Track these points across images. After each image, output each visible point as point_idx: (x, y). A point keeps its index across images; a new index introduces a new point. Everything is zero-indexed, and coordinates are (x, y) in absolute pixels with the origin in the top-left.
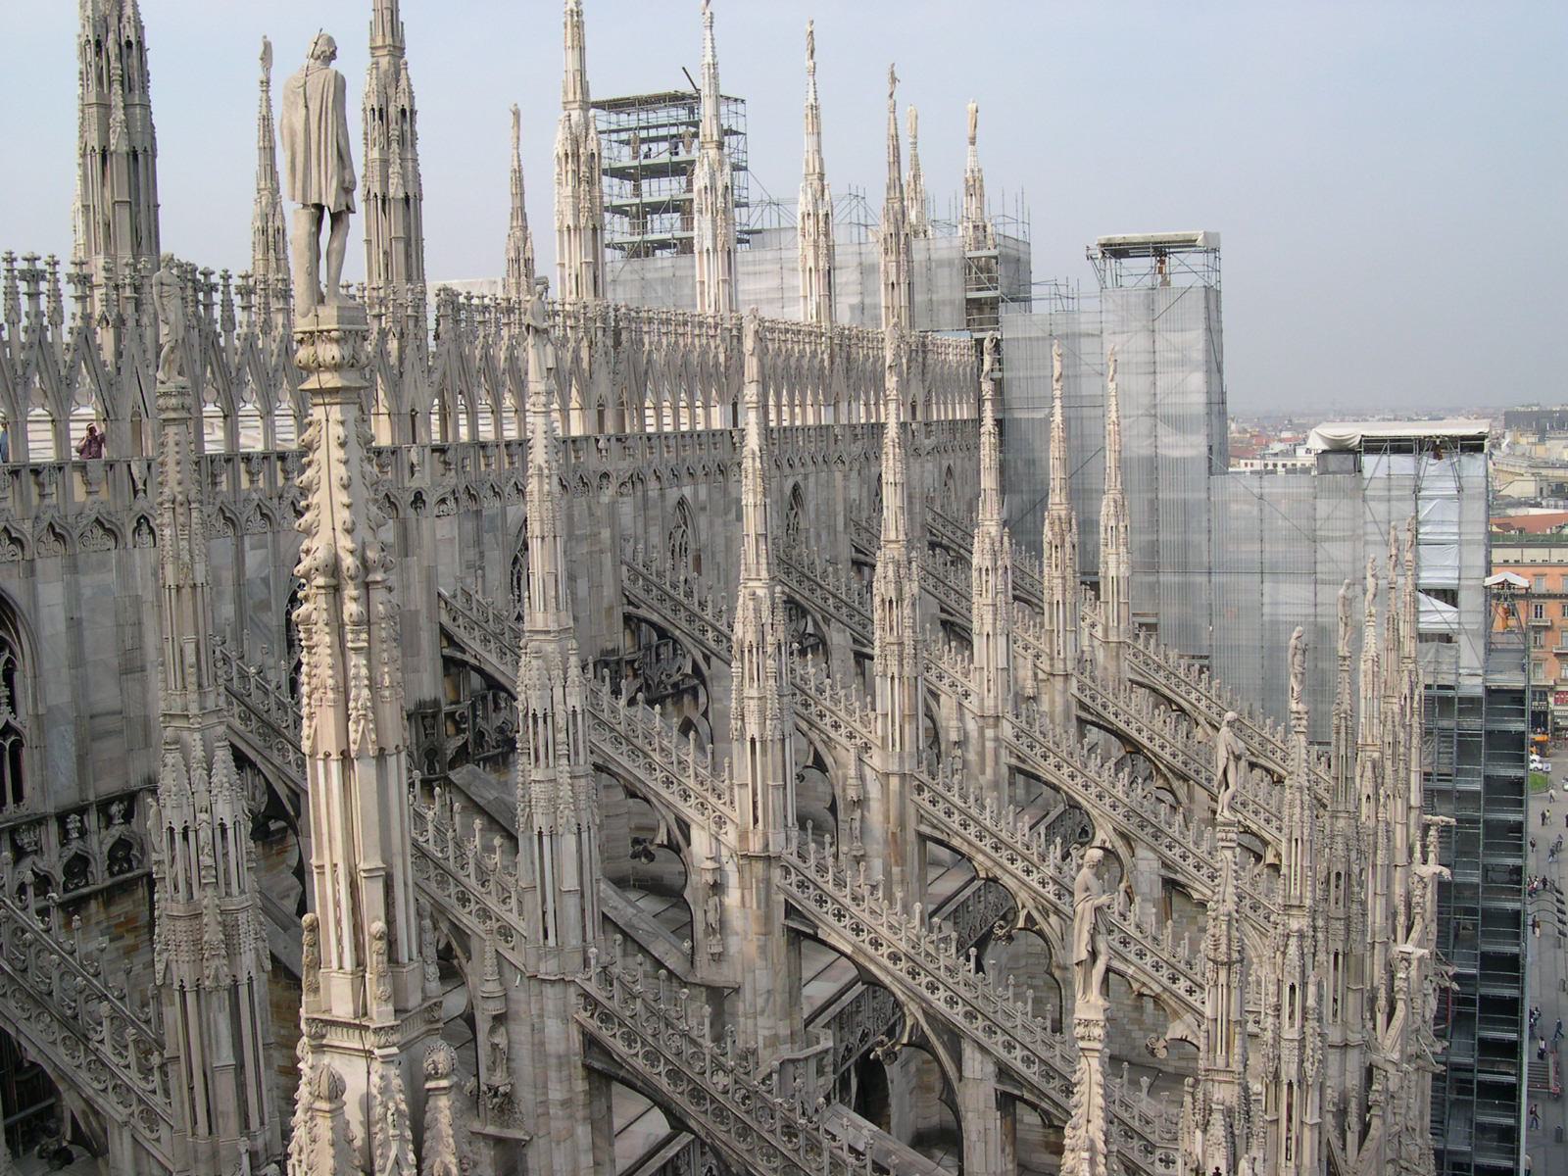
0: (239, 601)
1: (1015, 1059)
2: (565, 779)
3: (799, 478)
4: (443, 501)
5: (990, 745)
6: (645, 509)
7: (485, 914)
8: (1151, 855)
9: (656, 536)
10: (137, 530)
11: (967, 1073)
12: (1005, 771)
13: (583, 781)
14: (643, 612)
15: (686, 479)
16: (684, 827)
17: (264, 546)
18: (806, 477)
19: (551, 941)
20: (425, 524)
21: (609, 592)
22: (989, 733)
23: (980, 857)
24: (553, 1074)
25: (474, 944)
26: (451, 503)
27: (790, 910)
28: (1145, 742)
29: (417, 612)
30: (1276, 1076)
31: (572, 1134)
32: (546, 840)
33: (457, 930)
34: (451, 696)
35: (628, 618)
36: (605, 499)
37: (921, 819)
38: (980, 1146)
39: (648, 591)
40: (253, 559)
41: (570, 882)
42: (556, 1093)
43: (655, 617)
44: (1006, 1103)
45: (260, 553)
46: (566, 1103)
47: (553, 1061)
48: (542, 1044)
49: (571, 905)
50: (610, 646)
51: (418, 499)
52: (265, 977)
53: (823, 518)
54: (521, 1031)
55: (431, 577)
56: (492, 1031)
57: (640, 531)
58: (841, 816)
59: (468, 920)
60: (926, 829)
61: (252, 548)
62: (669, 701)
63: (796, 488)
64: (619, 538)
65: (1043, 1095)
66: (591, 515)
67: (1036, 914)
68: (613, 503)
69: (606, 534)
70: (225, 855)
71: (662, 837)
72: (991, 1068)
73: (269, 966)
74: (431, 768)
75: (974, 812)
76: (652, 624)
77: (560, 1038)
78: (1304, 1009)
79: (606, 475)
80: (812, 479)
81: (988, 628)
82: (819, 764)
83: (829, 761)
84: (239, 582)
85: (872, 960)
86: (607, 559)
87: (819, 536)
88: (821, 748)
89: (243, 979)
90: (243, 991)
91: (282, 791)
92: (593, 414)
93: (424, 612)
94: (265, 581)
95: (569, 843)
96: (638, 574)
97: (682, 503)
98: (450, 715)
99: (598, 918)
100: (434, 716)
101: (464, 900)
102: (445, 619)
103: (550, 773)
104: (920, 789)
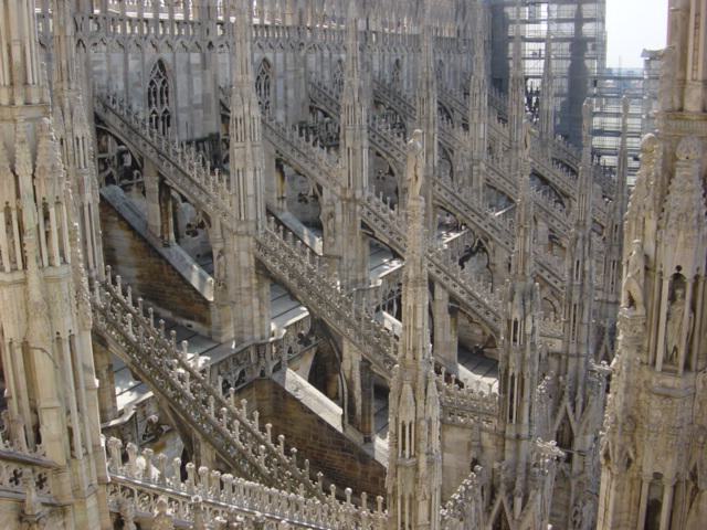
0: (126, 81)
1: (457, 290)
2: (248, 146)
3: (400, 58)
4: (222, 46)
5: (475, 173)
6: (322, 61)
7: (216, 207)
8: (543, 224)
9: (326, 73)
10: (78, 45)
11: (437, 297)
12: (481, 185)
13: (258, 148)
14: (318, 105)
15: (343, 51)
16: (320, 188)
17: (137, 59)
18: (403, 57)
19: (243, 218)
20: (213, 55)
21: (303, 96)
22: (475, 168)
23: (459, 215)
24: (243, 276)
25: (212, 220)
26: (225, 47)
27: (364, 225)
28: (550, 179)
29: (209, 95)
30: (570, 302)
31: (251, 303)
32: (241, 173)
33: (205, 215)
34: (225, 132)
35: (311, 108)
36: (303, 53)
37: (434, 198)
38: (441, 330)
39: (320, 95)
40: (132, 64)
41: (250, 190)
42: (245, 284)
43: (322, 107)
44: (453, 311)
45: (136, 62)
46: (249, 289)
47: (243, 270)
48: (239, 263)
49: (251, 201)
50: (303, 119)
51: (210, 45)
52: (97, 205)
53: (411, 77)
54: (229, 257)
55: (215, 80)
56: (219, 257)
57: (319, 69)
58: (400, 196)
59: (210, 208)
60: (436, 202)
61: (133, 58)
62: (332, 149)
63: (397, 61)
64: (308, 73)
65: (469, 307)
66: (295, 61)
67: (483, 242)
68: (305, 57)
69: (302, 70)
70: (79, 152)
71: (311, 193)
72: (446, 295)
73: (98, 200)
74: (215, 162)
75: (457, 194)
76: (322, 111)
77: (247, 260)
78: (584, 272)
79: (302, 44)
80: (406, 58)
81: (476, 120)
82: (391, 173)
83: (395, 171)
84: (126, 73)
85: (398, 247)
86: (303, 81)
87: (408, 84)
88: (393, 166)
89: (86, 203)
90: (86, 209)
91: (137, 158)
92: (297, 16)
93: (213, 94)
94: (139, 73)
95: (250, 175)
96: (315, 88)
97: (340, 61)
98: (224, 140)
99: (264, 210)
100: (217, 141)
101: (208, 201)
102: (222, 97)
103: (242, 144)
104: (434, 184)
